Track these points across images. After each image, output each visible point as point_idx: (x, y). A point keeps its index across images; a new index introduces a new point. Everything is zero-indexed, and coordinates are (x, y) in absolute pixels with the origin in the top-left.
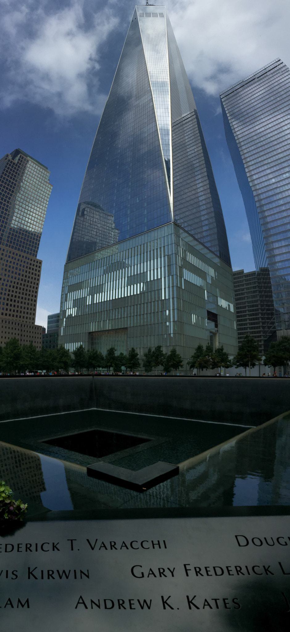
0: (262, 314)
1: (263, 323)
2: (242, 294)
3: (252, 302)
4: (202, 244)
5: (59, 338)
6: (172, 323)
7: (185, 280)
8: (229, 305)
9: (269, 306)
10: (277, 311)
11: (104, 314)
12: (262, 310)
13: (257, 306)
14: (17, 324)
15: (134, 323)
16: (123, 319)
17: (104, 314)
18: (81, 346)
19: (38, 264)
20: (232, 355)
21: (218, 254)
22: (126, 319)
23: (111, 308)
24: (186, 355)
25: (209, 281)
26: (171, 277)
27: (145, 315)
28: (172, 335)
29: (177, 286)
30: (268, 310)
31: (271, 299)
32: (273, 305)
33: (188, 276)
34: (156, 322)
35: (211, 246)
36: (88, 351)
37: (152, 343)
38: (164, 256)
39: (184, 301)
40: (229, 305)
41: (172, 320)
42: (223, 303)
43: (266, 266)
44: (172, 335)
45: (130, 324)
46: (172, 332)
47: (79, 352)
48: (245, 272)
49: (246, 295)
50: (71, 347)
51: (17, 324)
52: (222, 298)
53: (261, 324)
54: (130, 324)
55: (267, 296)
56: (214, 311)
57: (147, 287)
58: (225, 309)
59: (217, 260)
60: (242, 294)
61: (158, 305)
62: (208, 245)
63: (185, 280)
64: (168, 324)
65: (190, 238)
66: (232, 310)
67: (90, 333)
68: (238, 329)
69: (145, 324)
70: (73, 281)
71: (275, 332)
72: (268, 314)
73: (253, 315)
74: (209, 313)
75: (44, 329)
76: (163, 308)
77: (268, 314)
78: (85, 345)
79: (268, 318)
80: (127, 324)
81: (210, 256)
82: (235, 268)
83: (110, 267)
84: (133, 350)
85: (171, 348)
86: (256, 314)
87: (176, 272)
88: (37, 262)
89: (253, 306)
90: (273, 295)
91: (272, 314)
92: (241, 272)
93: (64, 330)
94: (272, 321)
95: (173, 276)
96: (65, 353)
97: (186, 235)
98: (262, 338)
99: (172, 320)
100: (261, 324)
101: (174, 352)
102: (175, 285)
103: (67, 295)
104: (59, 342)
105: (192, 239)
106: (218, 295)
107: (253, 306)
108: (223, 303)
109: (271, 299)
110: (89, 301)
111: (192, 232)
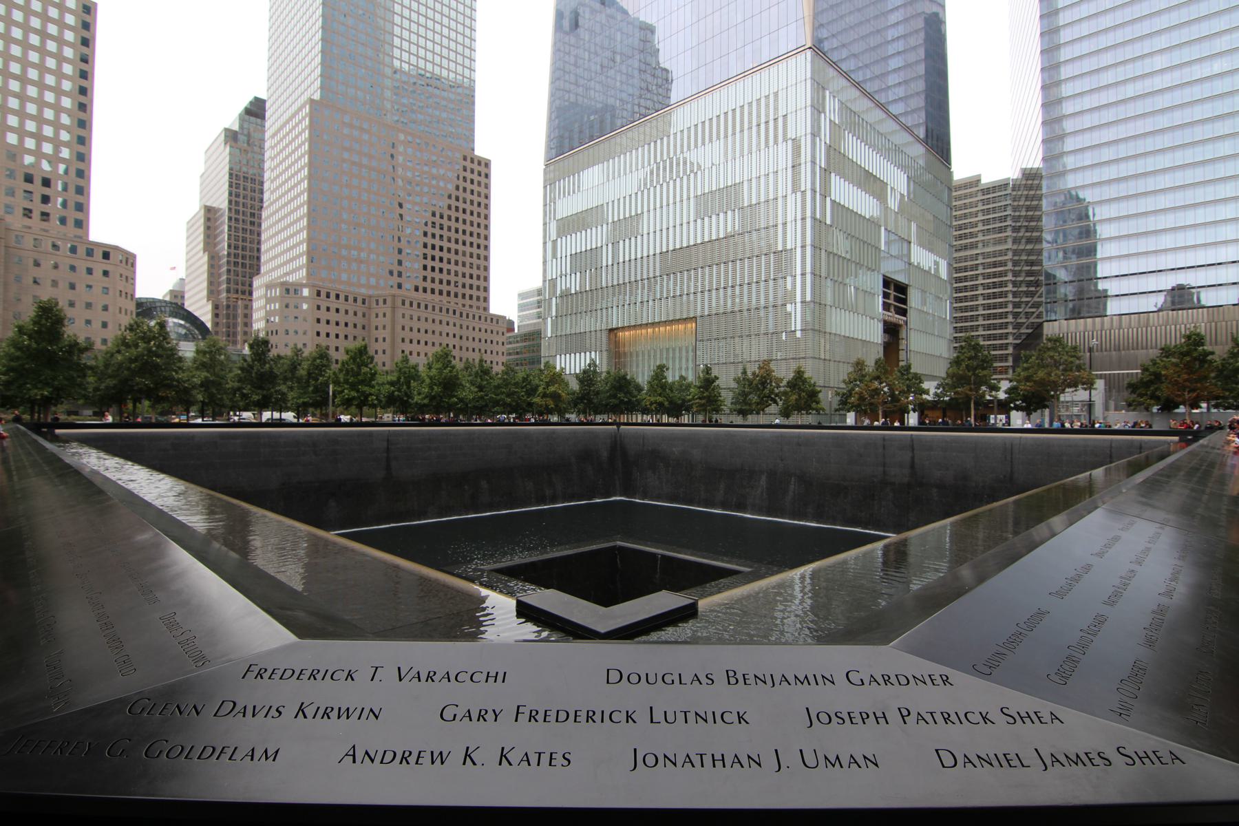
0: (1015, 284)
1: (1016, 305)
2: (972, 235)
3: (995, 254)
4: (882, 107)
5: (544, 343)
6: (799, 305)
7: (833, 202)
8: (936, 263)
9: (1032, 263)
10: (1049, 276)
11: (643, 288)
12: (1016, 274)
13: (1003, 264)
14: (451, 312)
15: (710, 307)
16: (685, 297)
17: (643, 288)
18: (593, 363)
19: (483, 170)
20: (933, 378)
21: (921, 133)
22: (692, 296)
23: (658, 274)
24: (830, 379)
25: (893, 204)
26: (799, 194)
27: (737, 288)
28: (798, 334)
29: (814, 218)
30: (1029, 273)
31: (1037, 247)
32: (1039, 263)
33: (845, 192)
34: (762, 302)
35: (905, 114)
36: (608, 373)
37: (752, 353)
38: (785, 140)
39: (829, 253)
40: (936, 263)
41: (798, 299)
42: (922, 257)
43: (1036, 166)
44: (798, 334)
45: (703, 308)
46: (799, 327)
47: (587, 377)
48: (983, 181)
49: (980, 238)
50: (571, 364)
51: (451, 312)
52: (921, 245)
53: (1010, 308)
54: (703, 308)
55: (1029, 241)
56: (901, 278)
57: (743, 218)
58: (928, 272)
59: (918, 151)
60: (972, 235)
61: (768, 264)
62: (896, 109)
63: (833, 202)
64: (789, 307)
65: (855, 93)
66: (944, 274)
67: (611, 330)
68: (957, 320)
69: (736, 309)
70: (568, 207)
71: (1040, 325)
72: (1029, 284)
73: (995, 285)
74: (887, 282)
75: (511, 323)
76: (778, 269)
77: (1029, 284)
78: (601, 359)
79: (1027, 294)
80: (696, 310)
81: (902, 138)
82: (961, 169)
83: (652, 173)
84: (708, 370)
85: (794, 366)
86: (1001, 284)
87: (813, 183)
88: (479, 163)
89: (995, 265)
90: (1044, 235)
91: (1037, 284)
92: (976, 181)
93: (554, 324)
94: (1036, 299)
95: (804, 192)
96: (557, 378)
97: (843, 82)
98: (1010, 340)
99: (798, 299)
100: (1010, 308)
101: (799, 374)
102: (808, 214)
103: (555, 242)
104: (544, 352)
105: (858, 93)
106: (913, 239)
107: (995, 265)
108: (922, 257)
109: (1037, 247)
110: (606, 258)
111: (859, 77)
